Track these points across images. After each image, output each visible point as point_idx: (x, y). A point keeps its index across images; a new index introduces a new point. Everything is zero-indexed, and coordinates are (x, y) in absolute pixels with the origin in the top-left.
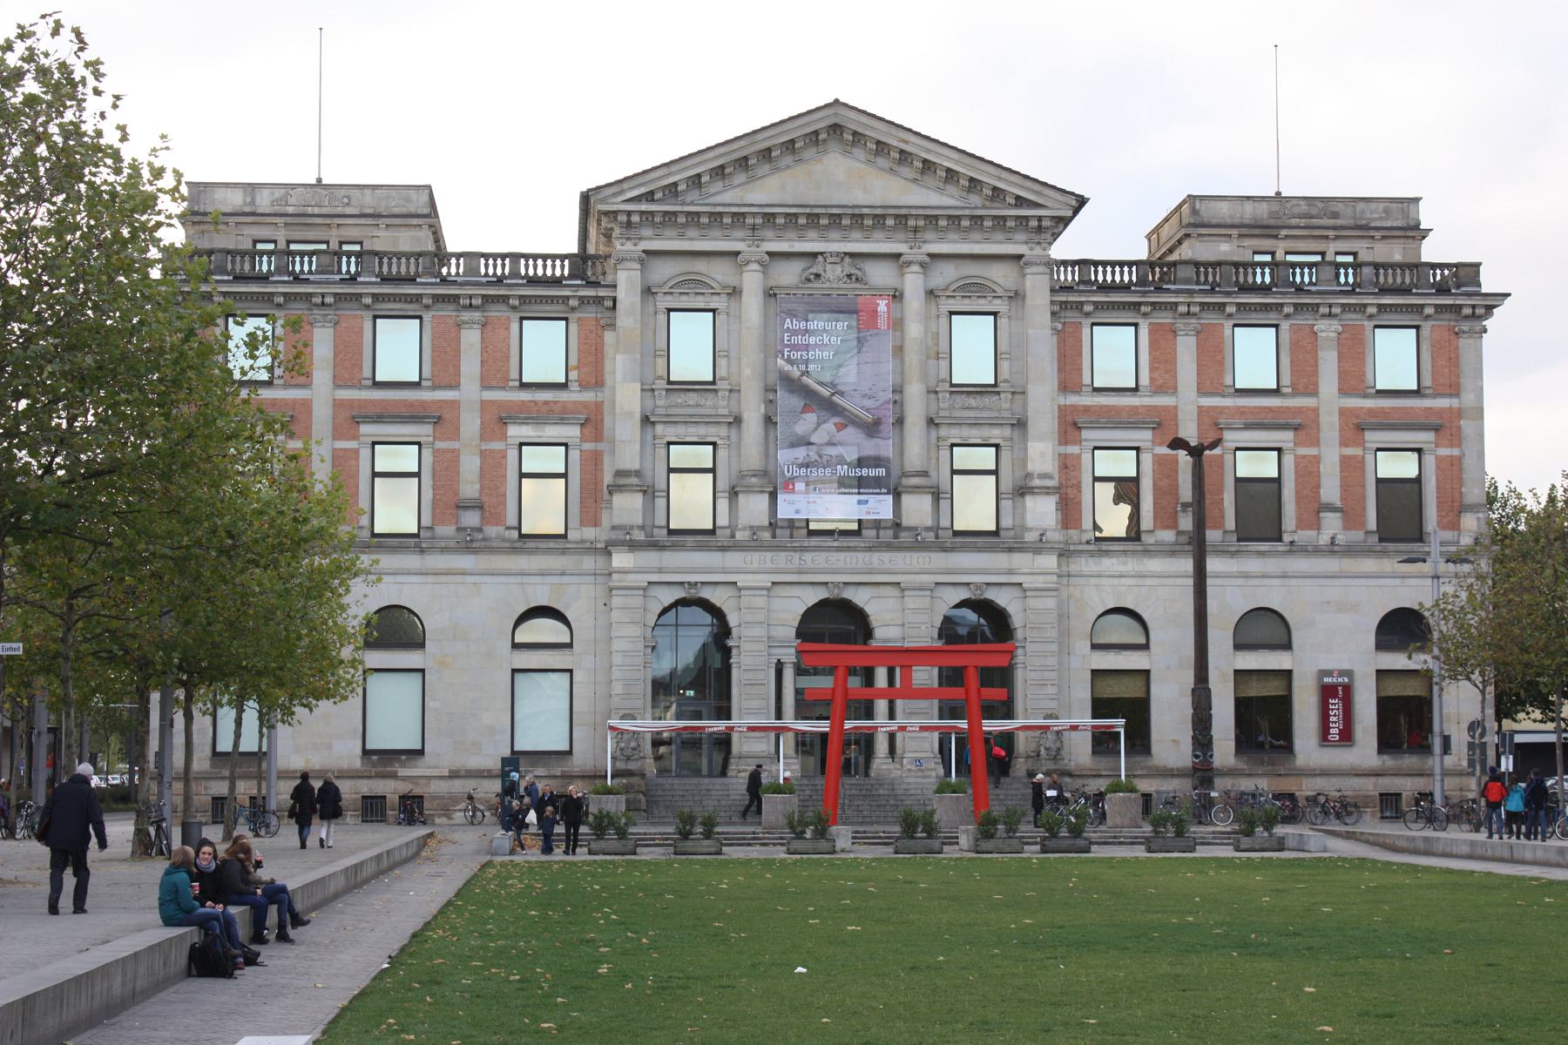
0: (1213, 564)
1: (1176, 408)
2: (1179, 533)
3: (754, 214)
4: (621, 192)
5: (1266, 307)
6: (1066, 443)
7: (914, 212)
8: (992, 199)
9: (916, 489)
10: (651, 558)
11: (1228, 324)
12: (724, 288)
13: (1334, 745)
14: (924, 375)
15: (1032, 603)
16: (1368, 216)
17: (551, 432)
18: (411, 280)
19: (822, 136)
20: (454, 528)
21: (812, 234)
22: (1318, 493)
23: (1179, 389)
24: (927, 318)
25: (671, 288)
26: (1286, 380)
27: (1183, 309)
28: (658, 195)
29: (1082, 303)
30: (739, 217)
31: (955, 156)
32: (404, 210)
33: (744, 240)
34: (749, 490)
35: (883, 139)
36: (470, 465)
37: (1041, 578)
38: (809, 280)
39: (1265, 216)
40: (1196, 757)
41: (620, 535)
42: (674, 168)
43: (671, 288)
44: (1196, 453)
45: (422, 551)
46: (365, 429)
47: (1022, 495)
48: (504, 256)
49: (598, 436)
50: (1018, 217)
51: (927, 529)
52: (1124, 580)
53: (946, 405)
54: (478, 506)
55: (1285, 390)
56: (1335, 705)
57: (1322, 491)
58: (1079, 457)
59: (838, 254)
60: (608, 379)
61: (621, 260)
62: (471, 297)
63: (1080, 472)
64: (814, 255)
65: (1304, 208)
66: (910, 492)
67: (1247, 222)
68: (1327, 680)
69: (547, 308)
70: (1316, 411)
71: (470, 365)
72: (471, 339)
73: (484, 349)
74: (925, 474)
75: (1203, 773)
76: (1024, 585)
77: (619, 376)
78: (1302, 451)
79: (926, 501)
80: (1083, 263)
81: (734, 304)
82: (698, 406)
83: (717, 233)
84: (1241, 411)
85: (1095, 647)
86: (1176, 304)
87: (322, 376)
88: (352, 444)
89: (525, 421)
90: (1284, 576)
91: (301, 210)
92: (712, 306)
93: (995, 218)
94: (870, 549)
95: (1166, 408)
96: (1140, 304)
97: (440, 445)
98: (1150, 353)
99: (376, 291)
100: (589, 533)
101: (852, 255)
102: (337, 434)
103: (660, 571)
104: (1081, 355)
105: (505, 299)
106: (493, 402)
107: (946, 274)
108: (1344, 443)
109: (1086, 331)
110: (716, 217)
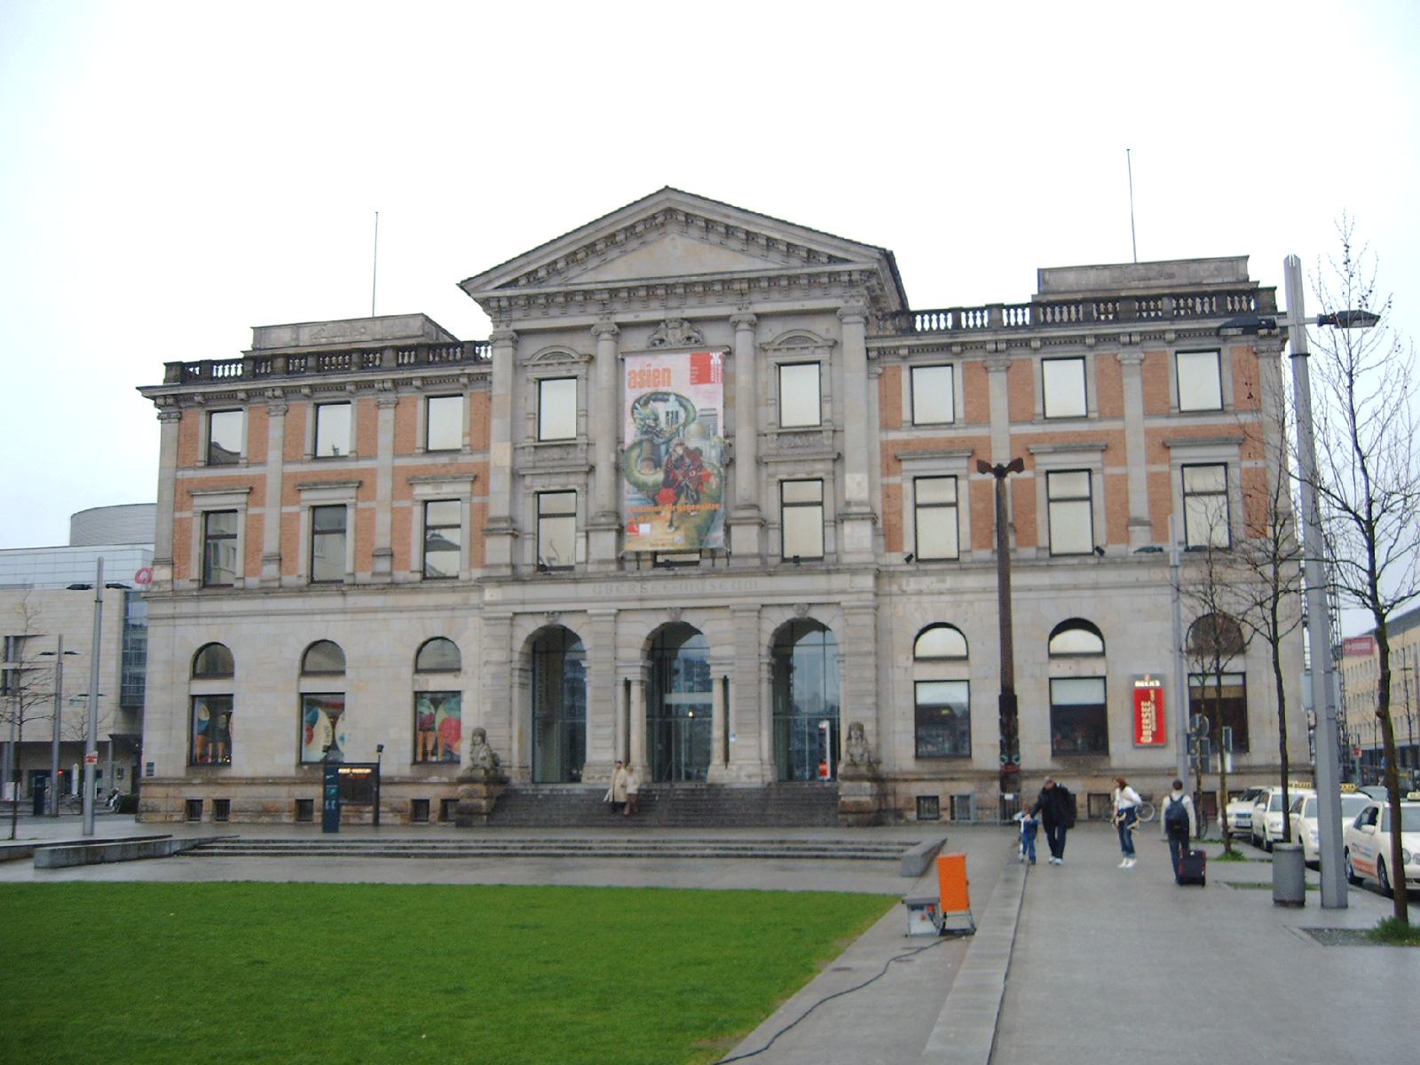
0: (1016, 580)
1: (989, 437)
4: (490, 282)
5: (1070, 340)
6: (888, 475)
7: (736, 276)
9: (742, 522)
10: (515, 592)
11: (1036, 359)
12: (581, 356)
13: (1149, 746)
14: (754, 419)
15: (852, 620)
16: (1202, 274)
17: (447, 490)
20: (370, 573)
22: (1127, 508)
23: (992, 420)
25: (539, 359)
26: (1093, 406)
27: (991, 347)
29: (898, 348)
32: (404, 334)
33: (596, 314)
36: (383, 521)
38: (655, 345)
39: (1108, 281)
40: (1002, 760)
42: (532, 257)
43: (539, 359)
44: (1000, 472)
46: (305, 495)
53: (774, 445)
55: (1090, 415)
56: (1148, 710)
57: (1131, 507)
58: (900, 487)
62: (383, 381)
63: (901, 499)
64: (656, 323)
65: (1142, 271)
67: (1091, 287)
68: (1139, 684)
69: (446, 386)
70: (1122, 432)
71: (385, 439)
75: (1009, 776)
76: (842, 604)
78: (1109, 470)
79: (755, 530)
82: (561, 459)
85: (916, 659)
87: (274, 455)
88: (295, 509)
89: (425, 482)
90: (1095, 587)
91: (331, 340)
92: (573, 373)
95: (980, 439)
96: (951, 344)
97: (361, 505)
98: (964, 389)
99: (310, 382)
101: (691, 321)
102: (284, 500)
103: (523, 603)
104: (900, 395)
106: (401, 468)
108: (1151, 460)
109: (905, 374)
110: (569, 296)
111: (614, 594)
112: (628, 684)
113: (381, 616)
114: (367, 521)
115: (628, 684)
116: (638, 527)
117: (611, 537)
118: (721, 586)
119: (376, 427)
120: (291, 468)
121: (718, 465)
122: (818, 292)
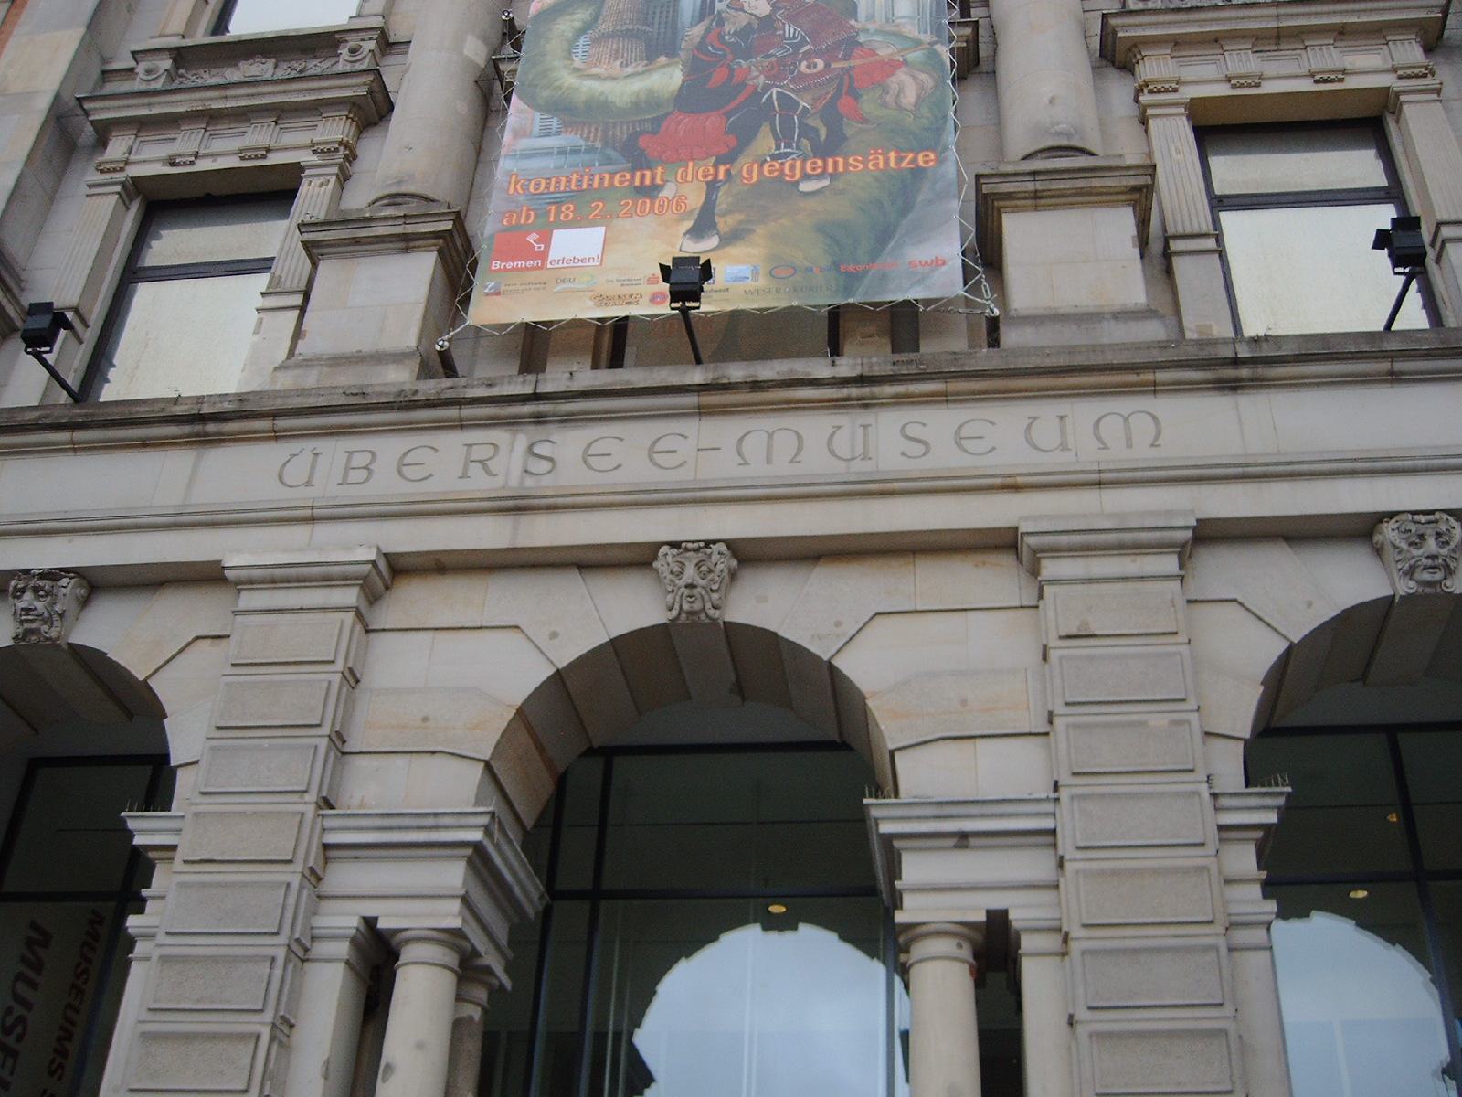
66: (1038, 200)
116: (546, 239)
118: (959, 439)
121: (926, 38)
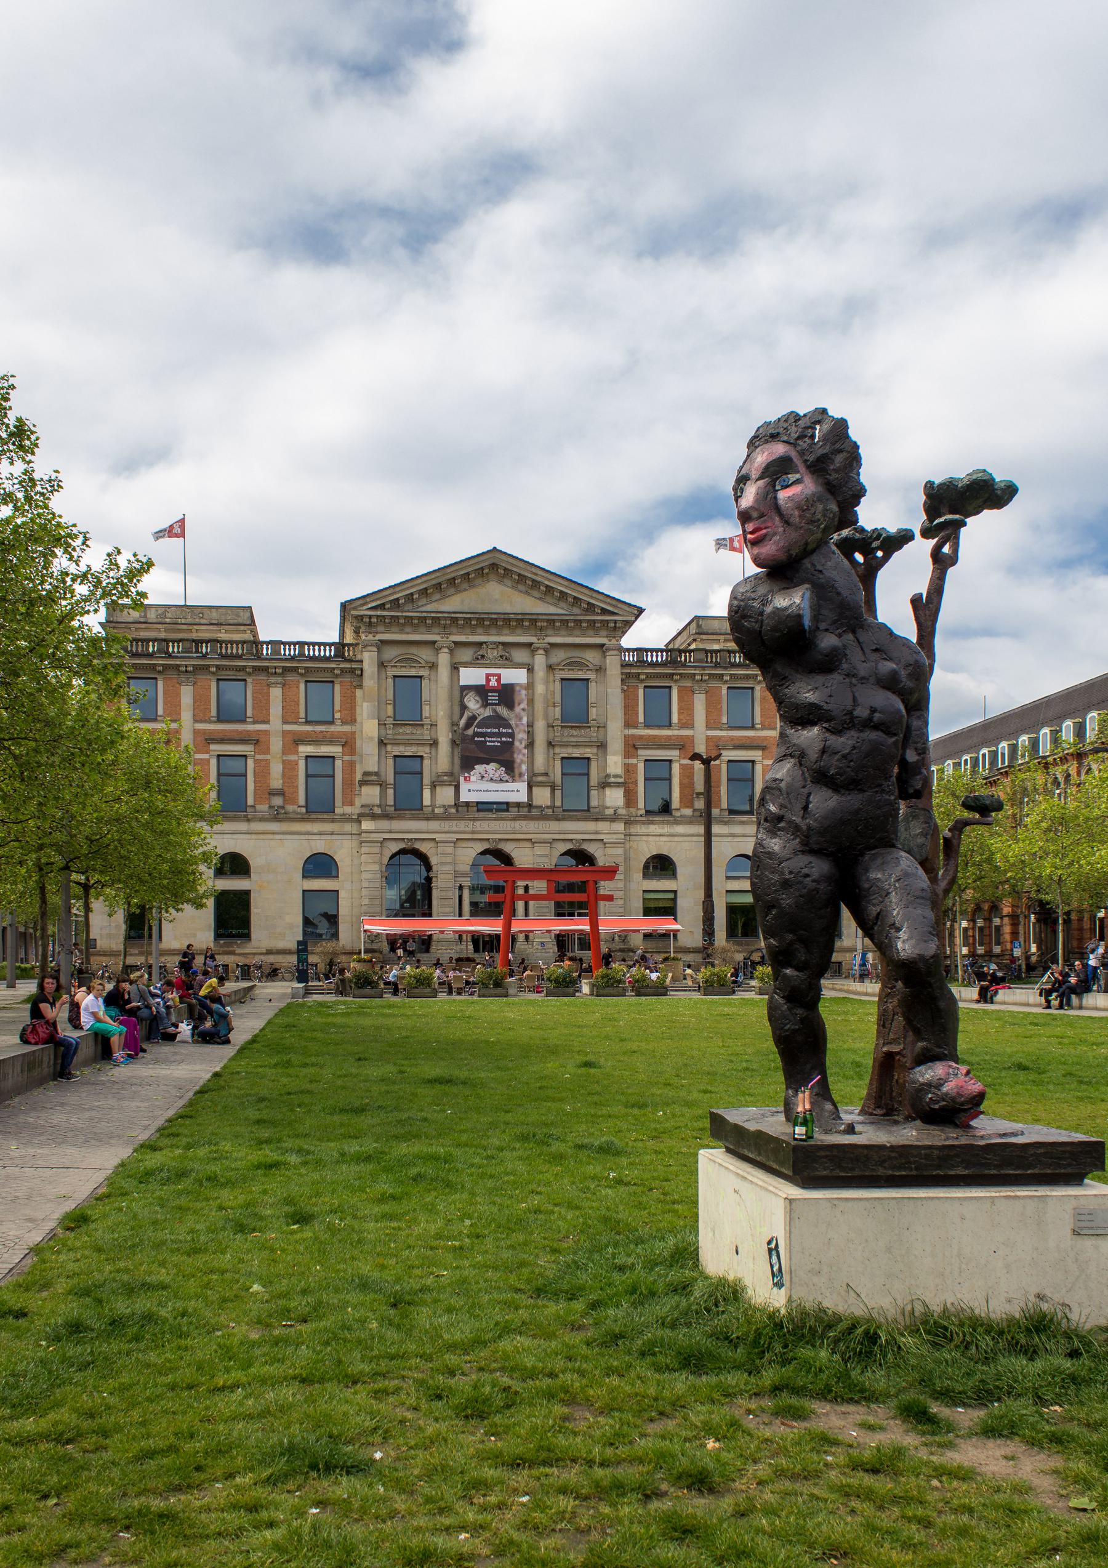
0: (716, 829)
2: (695, 810)
3: (445, 618)
8: (586, 610)
9: (541, 784)
10: (384, 824)
12: (427, 663)
14: (546, 716)
15: (609, 851)
18: (239, 657)
19: (486, 571)
21: (480, 630)
24: (547, 682)
27: (698, 677)
28: (388, 606)
29: (639, 674)
30: (436, 620)
31: (566, 583)
34: (443, 784)
35: (523, 573)
37: (615, 836)
41: (367, 811)
45: (249, 820)
46: (213, 747)
47: (603, 788)
48: (295, 644)
49: (353, 752)
50: (602, 621)
51: (548, 807)
52: (663, 838)
54: (281, 793)
58: (636, 765)
59: (495, 643)
60: (358, 719)
61: (365, 646)
64: (480, 644)
71: (276, 710)
72: (276, 693)
73: (284, 700)
74: (546, 774)
77: (365, 714)
79: (548, 791)
80: (639, 650)
81: (433, 674)
83: (422, 629)
84: (731, 738)
86: (694, 675)
87: (186, 716)
88: (206, 756)
92: (421, 674)
93: (588, 621)
94: (514, 819)
97: (258, 757)
100: (348, 810)
101: (504, 644)
103: (390, 832)
105: (296, 669)
107: (559, 656)
111: (455, 828)
112: (461, 888)
113: (277, 837)
114: (263, 770)
115: (461, 888)
117: (451, 791)
119: (268, 700)
120: (200, 726)
122: (591, 632)
